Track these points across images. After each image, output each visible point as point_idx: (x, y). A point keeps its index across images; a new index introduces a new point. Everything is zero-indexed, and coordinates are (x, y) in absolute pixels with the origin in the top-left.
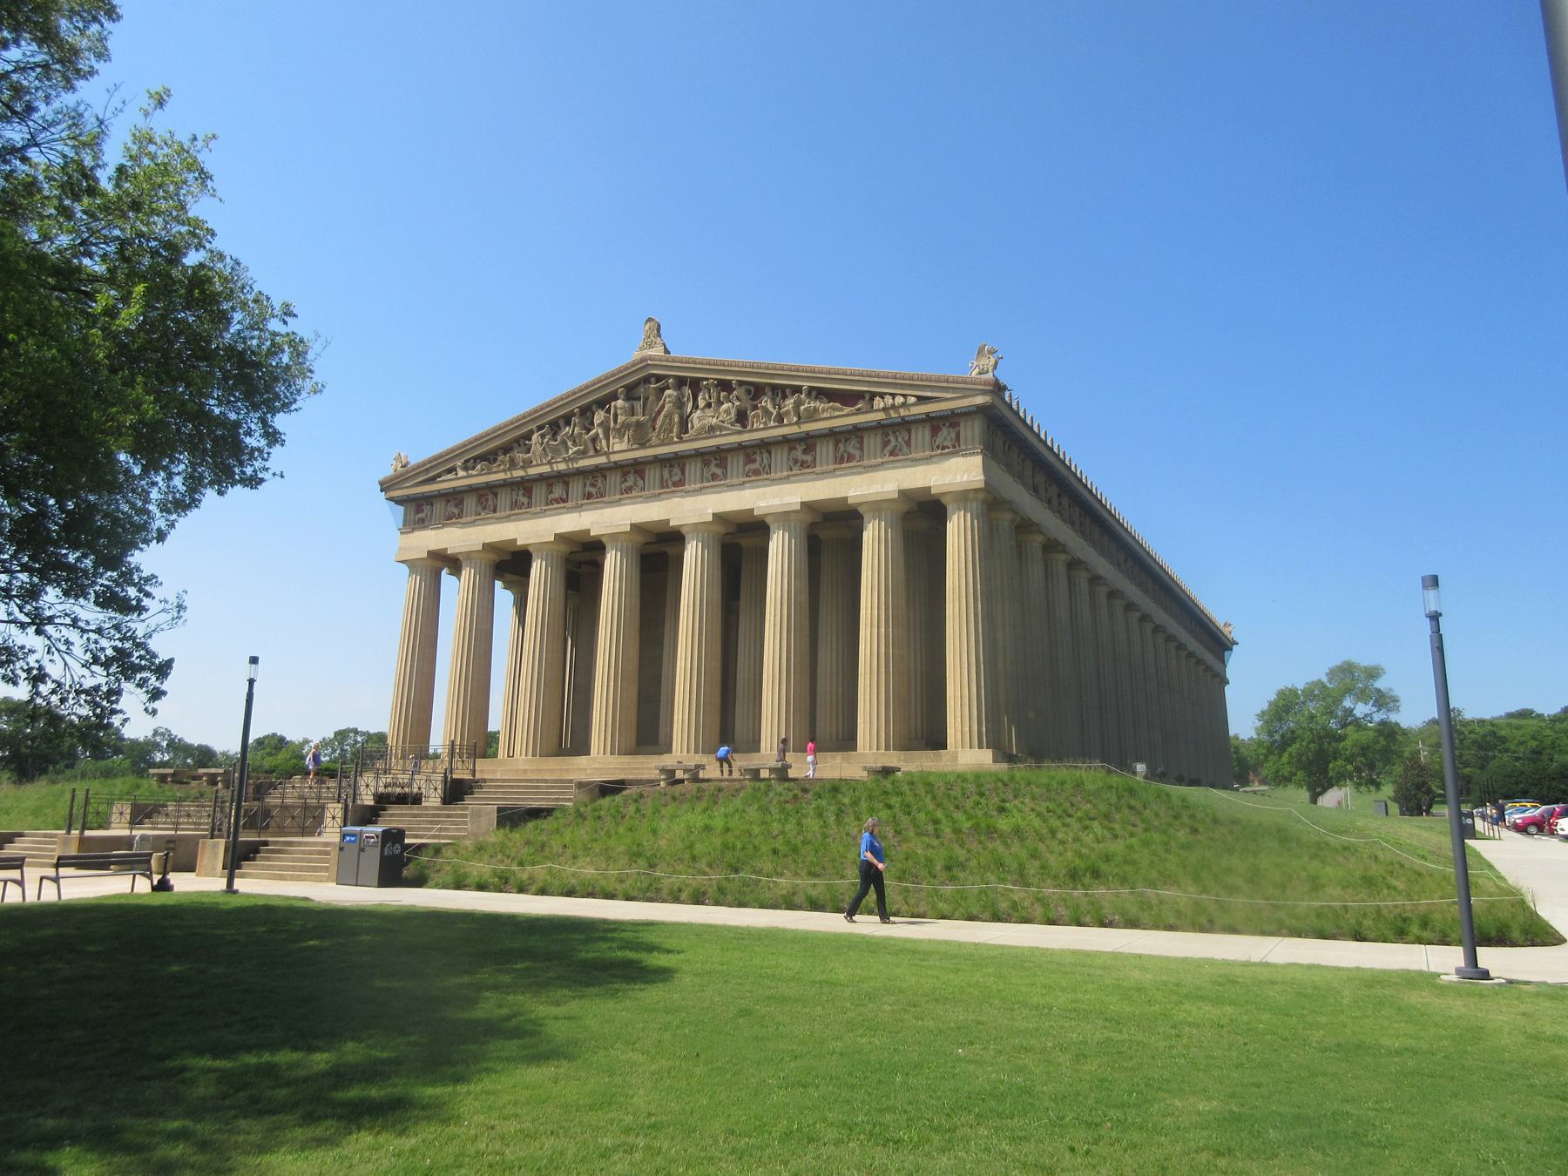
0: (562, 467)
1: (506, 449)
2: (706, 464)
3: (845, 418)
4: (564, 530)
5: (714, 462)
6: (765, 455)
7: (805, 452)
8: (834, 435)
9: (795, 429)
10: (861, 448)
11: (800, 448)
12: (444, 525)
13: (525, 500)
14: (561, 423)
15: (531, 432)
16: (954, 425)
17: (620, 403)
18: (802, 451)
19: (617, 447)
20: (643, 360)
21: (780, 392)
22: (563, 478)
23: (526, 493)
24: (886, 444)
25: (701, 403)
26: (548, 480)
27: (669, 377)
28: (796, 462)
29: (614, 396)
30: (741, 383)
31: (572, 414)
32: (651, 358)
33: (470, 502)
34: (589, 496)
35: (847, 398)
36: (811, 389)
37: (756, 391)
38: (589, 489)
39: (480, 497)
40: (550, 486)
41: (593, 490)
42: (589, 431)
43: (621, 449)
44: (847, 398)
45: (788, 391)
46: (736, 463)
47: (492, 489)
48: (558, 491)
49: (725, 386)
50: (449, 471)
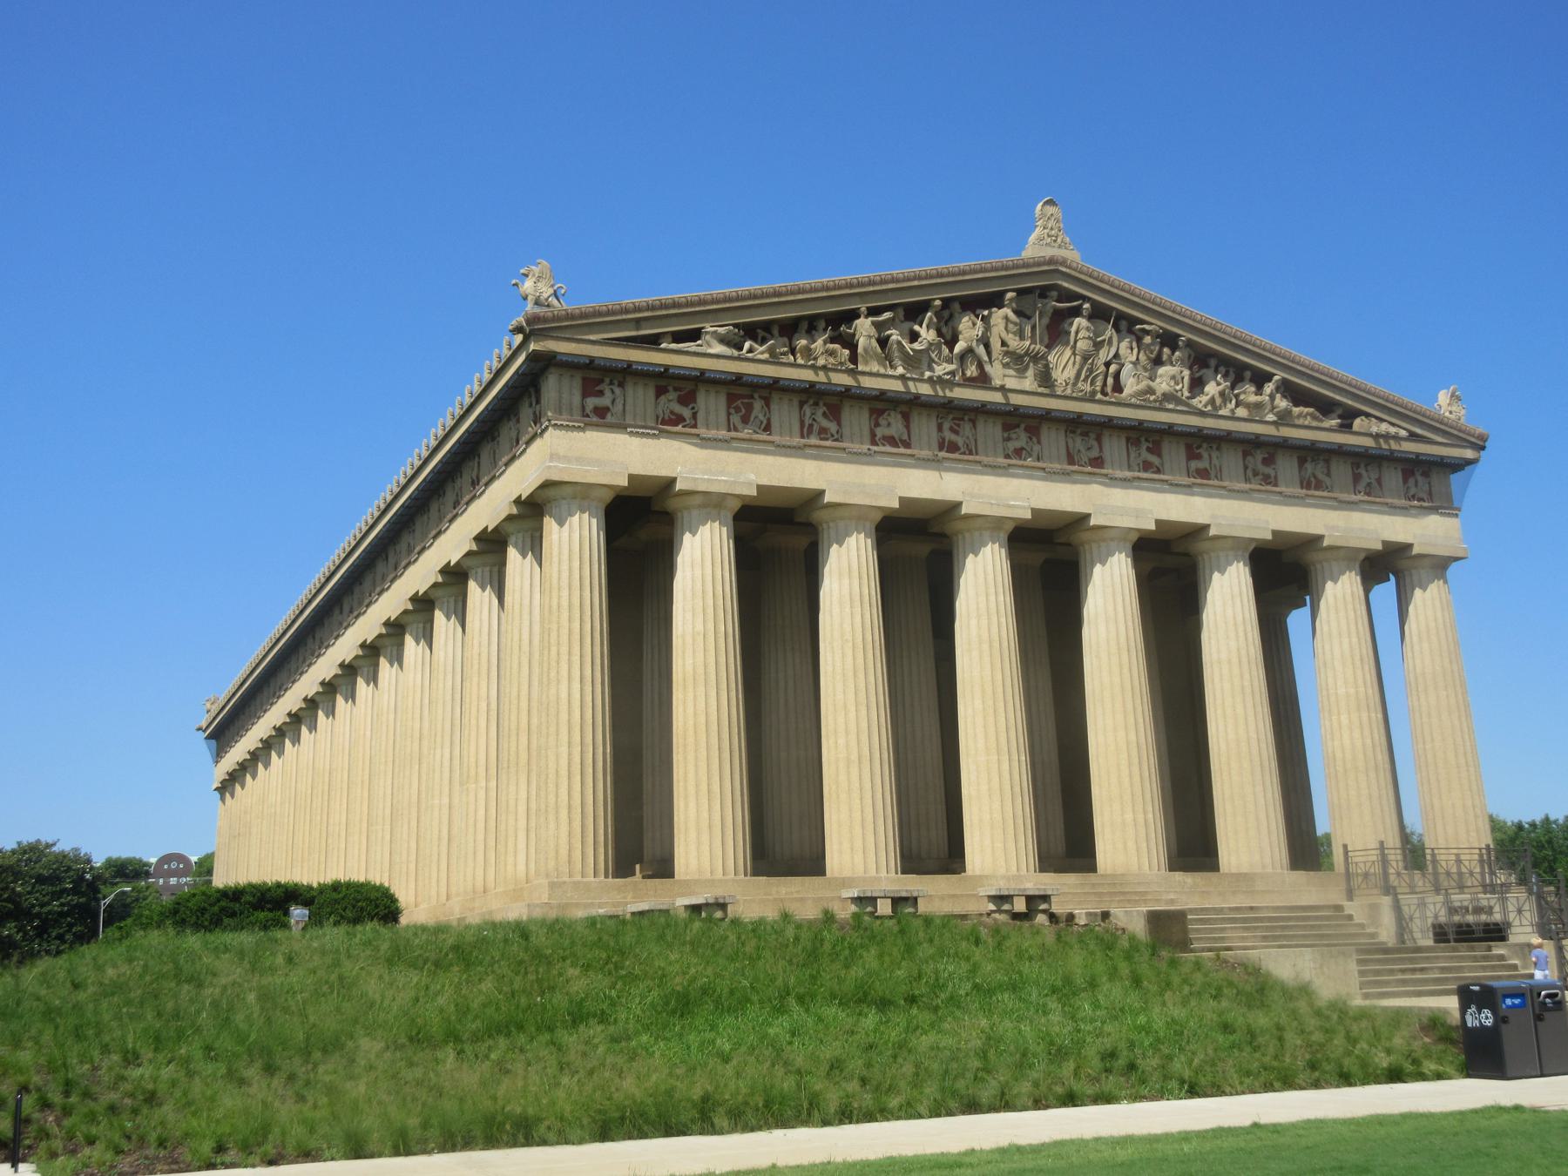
0: (925, 389)
1: (789, 329)
3: (1326, 433)
5: (1144, 445)
6: (1215, 454)
7: (1266, 462)
8: (1308, 453)
9: (1270, 431)
10: (1328, 475)
11: (1259, 456)
12: (588, 426)
13: (833, 427)
14: (901, 312)
15: (853, 315)
16: (1426, 474)
18: (1259, 460)
20: (1051, 261)
22: (908, 405)
23: (826, 411)
24: (1357, 478)
26: (881, 403)
27: (1085, 299)
28: (1256, 474)
29: (995, 300)
31: (923, 307)
32: (1064, 262)
33: (711, 404)
34: (953, 448)
38: (949, 436)
39: (731, 399)
40: (880, 412)
41: (960, 441)
42: (951, 343)
44: (1325, 407)
45: (1248, 374)
46: (1174, 454)
48: (895, 426)
49: (1169, 340)
50: (679, 337)
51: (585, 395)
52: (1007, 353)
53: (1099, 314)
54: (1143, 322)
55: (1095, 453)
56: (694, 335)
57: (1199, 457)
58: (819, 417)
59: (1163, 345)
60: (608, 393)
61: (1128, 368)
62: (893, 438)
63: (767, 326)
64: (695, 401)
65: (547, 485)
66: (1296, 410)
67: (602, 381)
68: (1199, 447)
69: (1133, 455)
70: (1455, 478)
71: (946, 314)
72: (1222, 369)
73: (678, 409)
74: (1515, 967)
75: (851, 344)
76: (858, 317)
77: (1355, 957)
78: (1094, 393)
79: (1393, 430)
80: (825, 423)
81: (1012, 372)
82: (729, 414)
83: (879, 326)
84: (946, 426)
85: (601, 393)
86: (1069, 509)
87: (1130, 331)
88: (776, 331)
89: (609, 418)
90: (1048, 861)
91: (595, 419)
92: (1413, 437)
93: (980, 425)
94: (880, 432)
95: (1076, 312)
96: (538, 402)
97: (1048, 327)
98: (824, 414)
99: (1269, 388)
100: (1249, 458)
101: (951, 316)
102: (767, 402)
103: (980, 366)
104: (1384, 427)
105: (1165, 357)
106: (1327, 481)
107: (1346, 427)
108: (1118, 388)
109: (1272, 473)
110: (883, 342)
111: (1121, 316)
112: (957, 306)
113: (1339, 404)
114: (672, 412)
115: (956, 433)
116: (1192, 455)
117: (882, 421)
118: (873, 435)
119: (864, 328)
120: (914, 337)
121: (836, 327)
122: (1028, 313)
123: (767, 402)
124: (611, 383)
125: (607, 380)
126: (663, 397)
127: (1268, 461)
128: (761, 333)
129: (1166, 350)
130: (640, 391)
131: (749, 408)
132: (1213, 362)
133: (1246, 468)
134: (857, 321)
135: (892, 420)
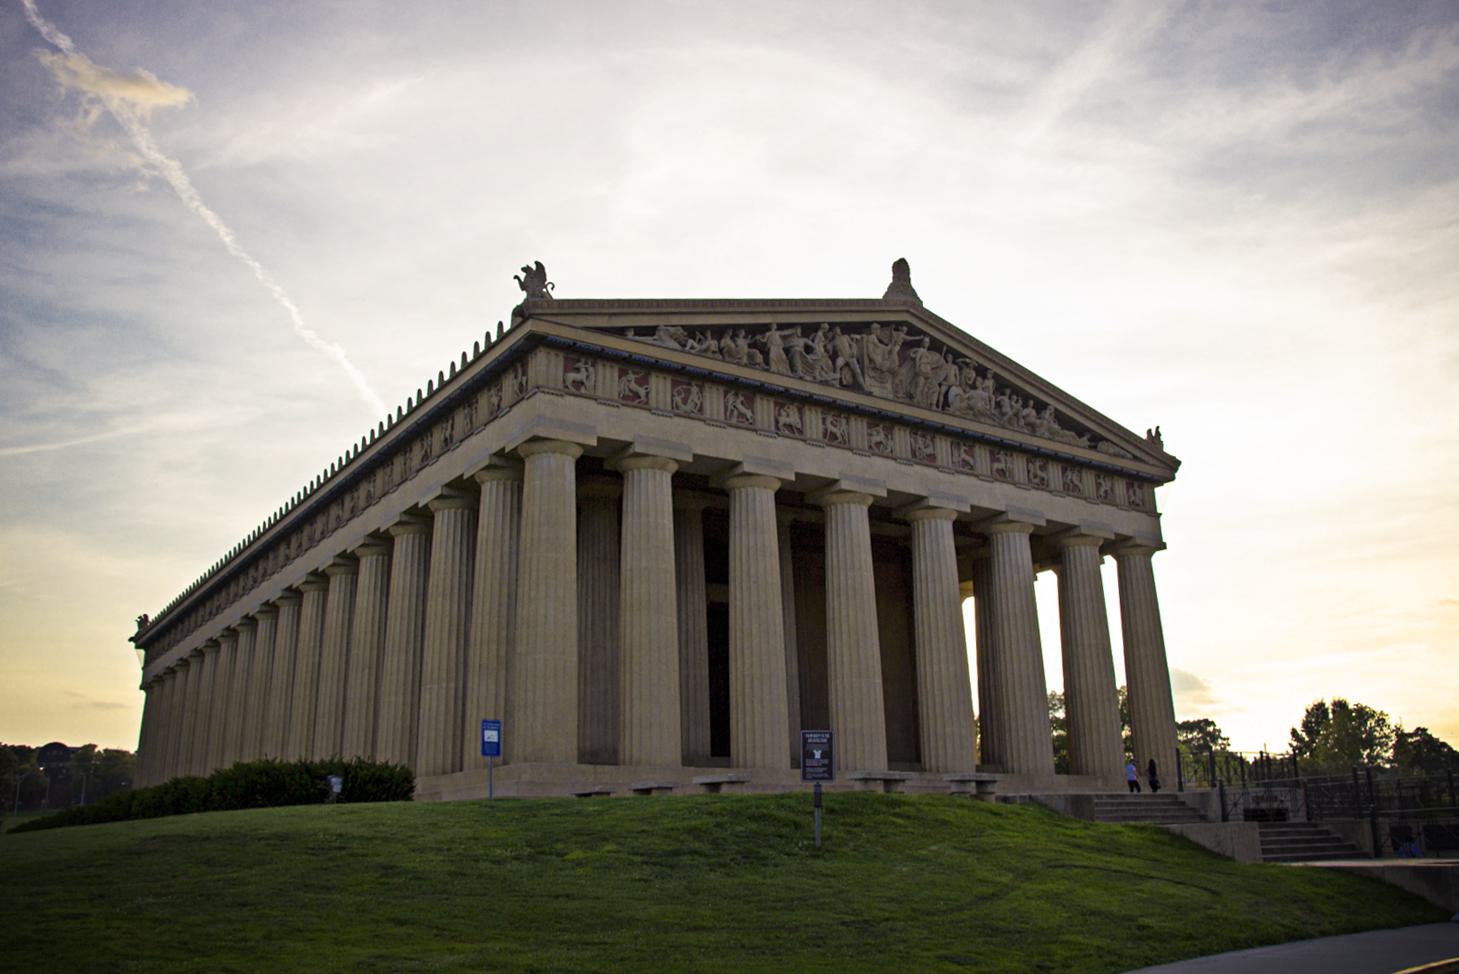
1: (719, 332)
2: (956, 445)
4: (806, 471)
5: (963, 448)
6: (1009, 459)
8: (1070, 463)
13: (749, 413)
17: (873, 337)
19: (876, 391)
21: (1026, 398)
22: (806, 401)
24: (1099, 485)
25: (952, 378)
30: (996, 376)
31: (816, 327)
35: (1081, 431)
36: (1056, 410)
37: (1001, 386)
39: (674, 384)
43: (880, 395)
44: (1081, 431)
45: (1031, 403)
47: (708, 378)
49: (982, 372)
50: (642, 331)
51: (566, 370)
52: (875, 369)
53: (936, 346)
54: (965, 357)
55: (929, 451)
56: (650, 331)
57: (999, 460)
58: (739, 406)
59: (977, 375)
60: (583, 370)
61: (954, 391)
62: (790, 426)
63: (703, 329)
64: (647, 383)
65: (535, 439)
66: (1061, 432)
67: (579, 361)
68: (998, 453)
69: (956, 453)
70: (1158, 491)
71: (830, 335)
72: (1015, 397)
73: (634, 386)
74: (1339, 840)
75: (765, 351)
76: (770, 330)
77: (1258, 831)
78: (931, 404)
79: (1122, 452)
80: (743, 410)
81: (876, 384)
82: (673, 396)
83: (784, 338)
84: (829, 419)
85: (578, 370)
86: (912, 491)
87: (954, 363)
88: (709, 335)
89: (583, 390)
90: (893, 759)
91: (572, 390)
92: (1135, 458)
93: (853, 418)
94: (783, 420)
95: (919, 344)
96: (524, 373)
97: (899, 354)
98: (742, 403)
99: (1047, 414)
100: (1031, 465)
101: (833, 338)
102: (701, 389)
103: (854, 375)
104: (1117, 449)
105: (978, 384)
106: (1080, 485)
107: (1094, 448)
108: (946, 404)
109: (1046, 478)
110: (787, 351)
111: (950, 350)
112: (838, 330)
113: (1089, 430)
114: (630, 390)
115: (835, 426)
116: (994, 459)
117: (783, 413)
118: (777, 422)
119: (775, 339)
120: (808, 349)
121: (754, 335)
122: (885, 341)
123: (701, 389)
124: (586, 363)
125: (583, 360)
126: (624, 379)
127: (1043, 468)
128: (699, 336)
129: (979, 379)
130: (608, 371)
131: (688, 392)
132: (1008, 391)
133: (1029, 472)
134: (768, 334)
135: (791, 413)
